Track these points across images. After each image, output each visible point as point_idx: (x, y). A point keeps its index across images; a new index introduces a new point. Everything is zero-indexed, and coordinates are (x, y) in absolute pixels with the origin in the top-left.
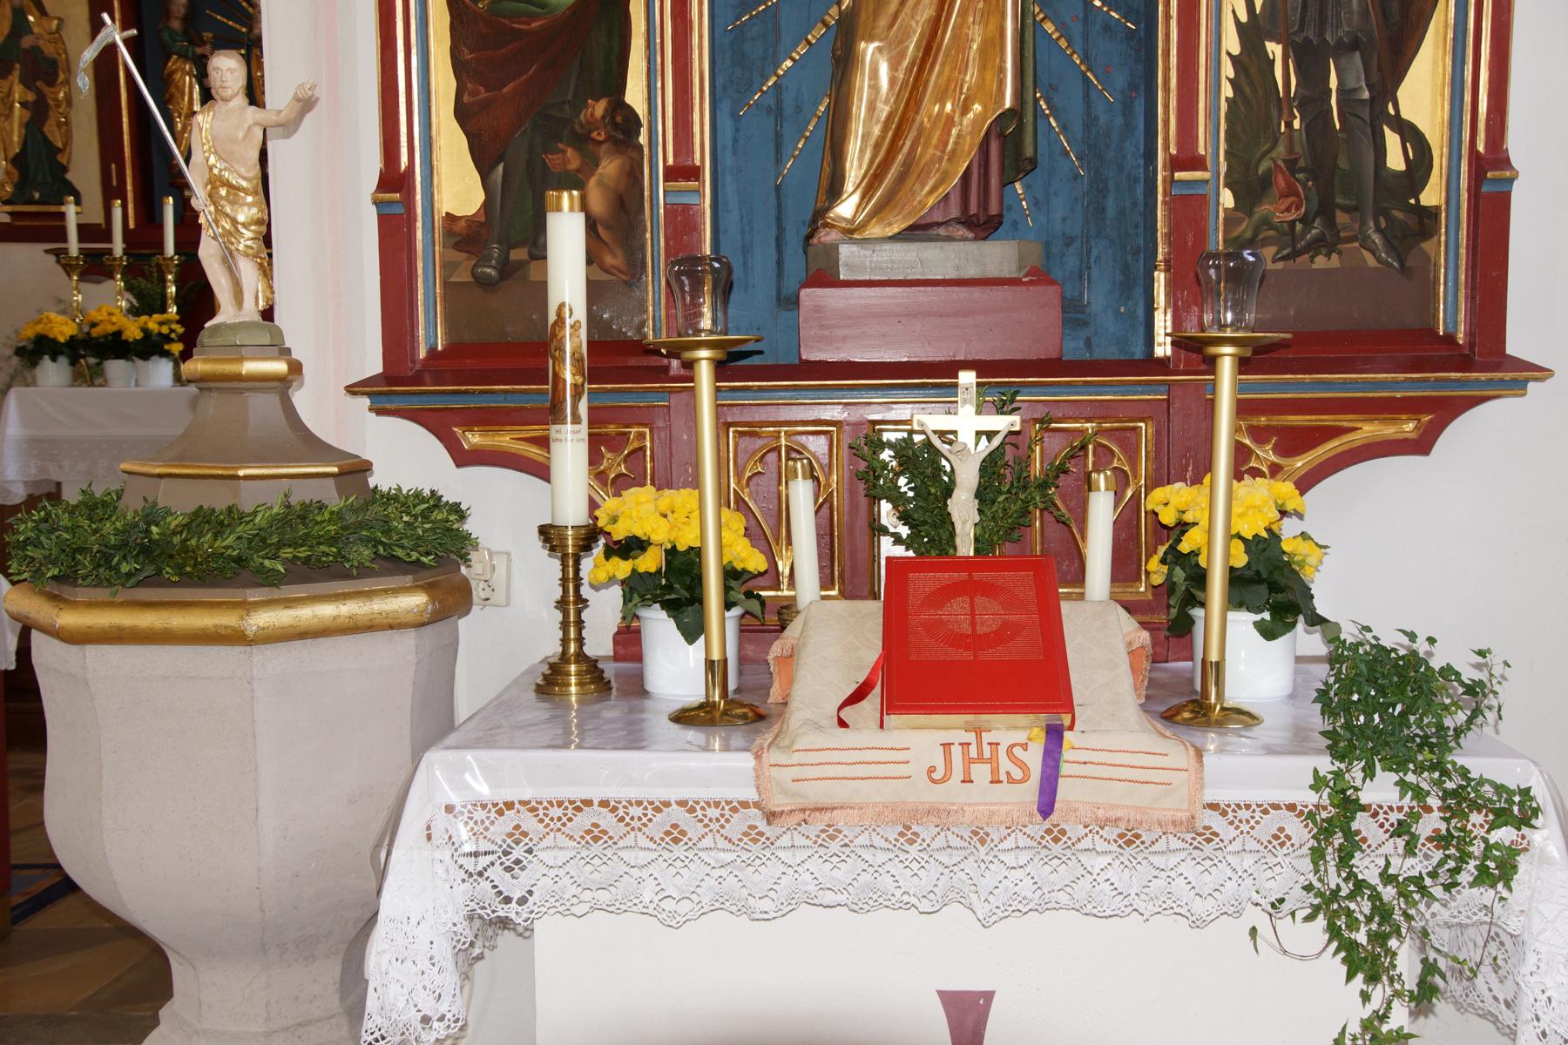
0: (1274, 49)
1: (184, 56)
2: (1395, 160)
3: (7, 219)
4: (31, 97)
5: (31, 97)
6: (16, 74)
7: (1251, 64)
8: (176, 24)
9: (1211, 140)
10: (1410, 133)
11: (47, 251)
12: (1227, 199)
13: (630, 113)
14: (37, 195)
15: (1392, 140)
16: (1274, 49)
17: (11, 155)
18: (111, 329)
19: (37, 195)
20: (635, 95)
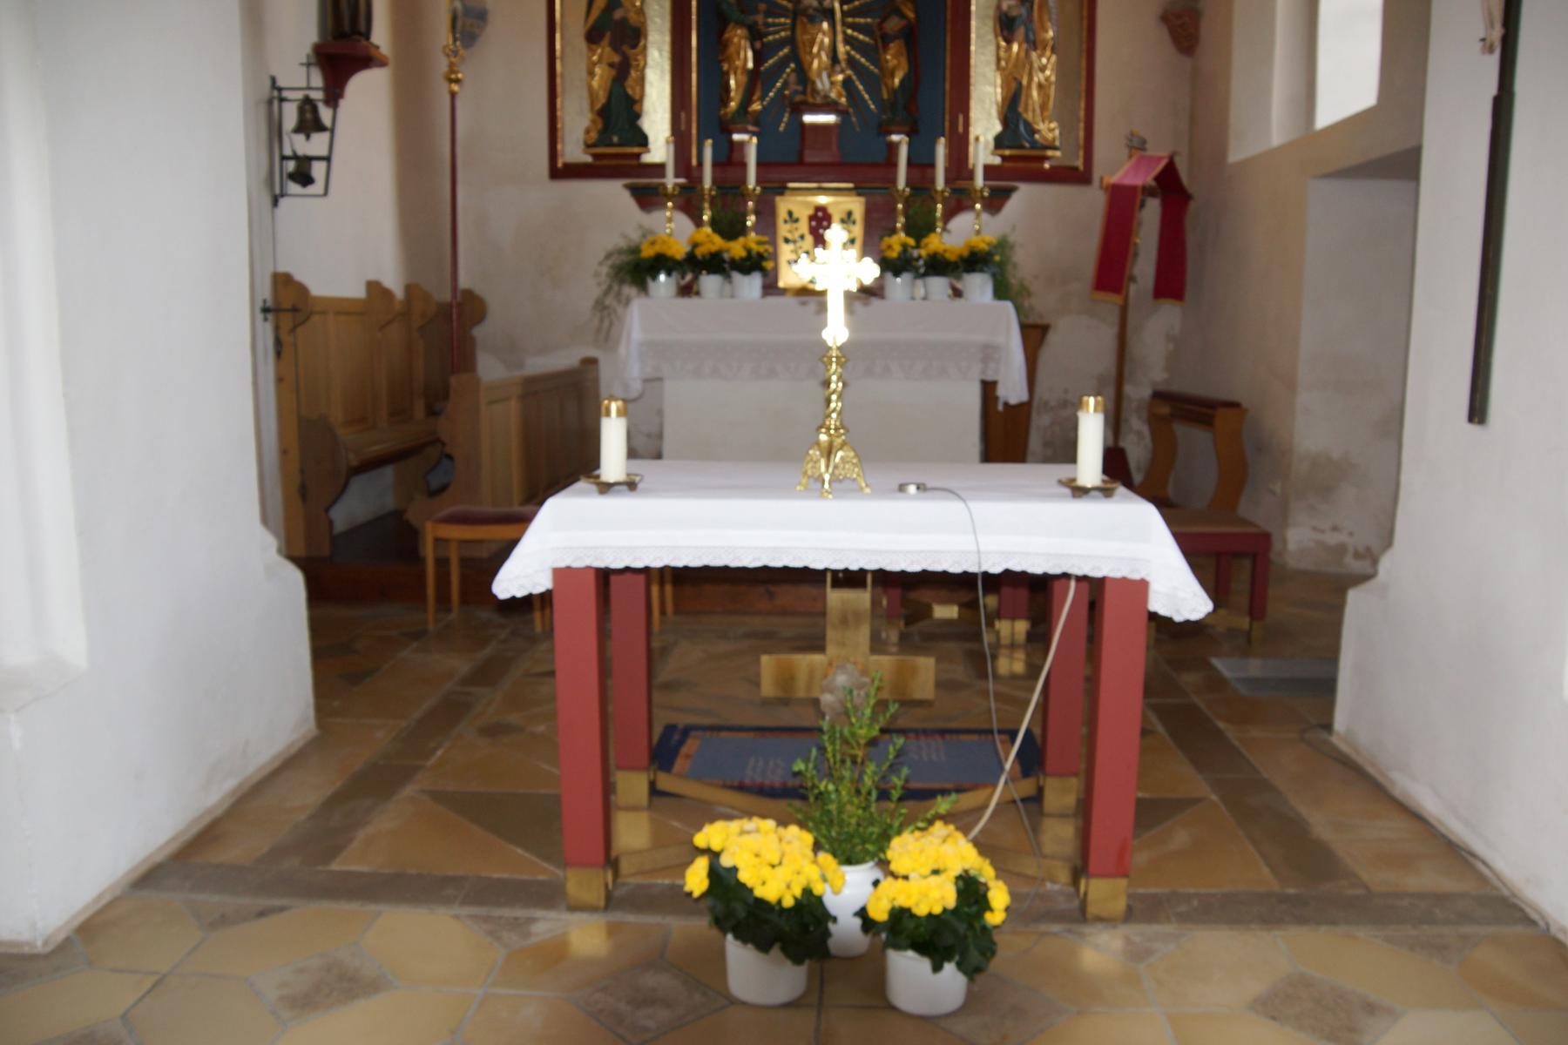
1: (740, 24)
3: (588, 159)
4: (616, 59)
5: (616, 59)
6: (608, 35)
11: (628, 187)
14: (615, 139)
17: (598, 106)
18: (714, 248)
19: (615, 139)
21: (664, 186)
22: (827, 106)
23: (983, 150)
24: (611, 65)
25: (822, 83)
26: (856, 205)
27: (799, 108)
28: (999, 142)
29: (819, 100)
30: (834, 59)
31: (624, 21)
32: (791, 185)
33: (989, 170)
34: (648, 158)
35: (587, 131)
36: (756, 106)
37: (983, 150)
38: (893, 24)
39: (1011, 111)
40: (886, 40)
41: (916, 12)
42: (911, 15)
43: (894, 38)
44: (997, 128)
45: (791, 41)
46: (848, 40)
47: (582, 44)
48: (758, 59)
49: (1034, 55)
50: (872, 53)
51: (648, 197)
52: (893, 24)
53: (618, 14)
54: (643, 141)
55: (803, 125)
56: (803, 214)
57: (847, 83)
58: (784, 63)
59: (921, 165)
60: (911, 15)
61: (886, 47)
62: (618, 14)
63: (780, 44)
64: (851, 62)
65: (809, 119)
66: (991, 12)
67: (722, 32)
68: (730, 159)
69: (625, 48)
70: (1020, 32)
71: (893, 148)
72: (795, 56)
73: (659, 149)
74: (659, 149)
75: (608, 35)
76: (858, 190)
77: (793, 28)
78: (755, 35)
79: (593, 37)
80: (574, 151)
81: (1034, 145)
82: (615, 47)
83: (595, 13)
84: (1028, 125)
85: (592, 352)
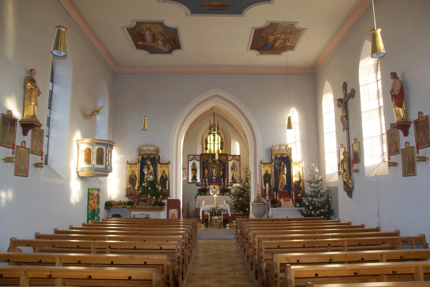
0: (296, 183)
1: (206, 169)
2: (300, 187)
3: (191, 182)
4: (194, 172)
5: (194, 172)
6: (194, 170)
7: (295, 183)
8: (205, 166)
9: (294, 186)
10: (301, 186)
12: (294, 188)
13: (271, 185)
15: (300, 186)
16: (296, 183)
17: (192, 177)
20: (271, 184)
21: (199, 185)
22: (215, 177)
23: (230, 181)
24: (194, 173)
25: (214, 175)
26: (218, 187)
27: (212, 177)
28: (232, 180)
29: (214, 176)
30: (215, 172)
31: (195, 168)
32: (212, 184)
33: (231, 183)
34: (197, 182)
35: (192, 179)
36: (208, 176)
37: (230, 181)
38: (221, 169)
39: (233, 177)
40: (220, 170)
41: (223, 167)
42: (223, 168)
43: (221, 170)
44: (231, 178)
45: (211, 170)
46: (217, 170)
47: (191, 171)
48: (208, 172)
49: (235, 171)
50: (219, 171)
51: (197, 185)
52: (221, 169)
53: (195, 168)
54: (197, 180)
55: (212, 178)
56: (213, 187)
57: (217, 174)
58: (210, 172)
59: (224, 182)
60: (223, 168)
61: (220, 171)
62: (195, 168)
63: (210, 170)
64: (217, 172)
65: (213, 178)
66: (231, 167)
67: (204, 169)
68: (205, 182)
69: (195, 171)
70: (233, 169)
71: (221, 180)
72: (211, 171)
73: (199, 181)
74: (199, 181)
75: (194, 170)
76: (218, 185)
77: (211, 169)
78: (208, 170)
79: (192, 170)
80: (190, 181)
81: (235, 180)
82: (194, 171)
83: (192, 168)
84: (234, 178)
85: (189, 201)
